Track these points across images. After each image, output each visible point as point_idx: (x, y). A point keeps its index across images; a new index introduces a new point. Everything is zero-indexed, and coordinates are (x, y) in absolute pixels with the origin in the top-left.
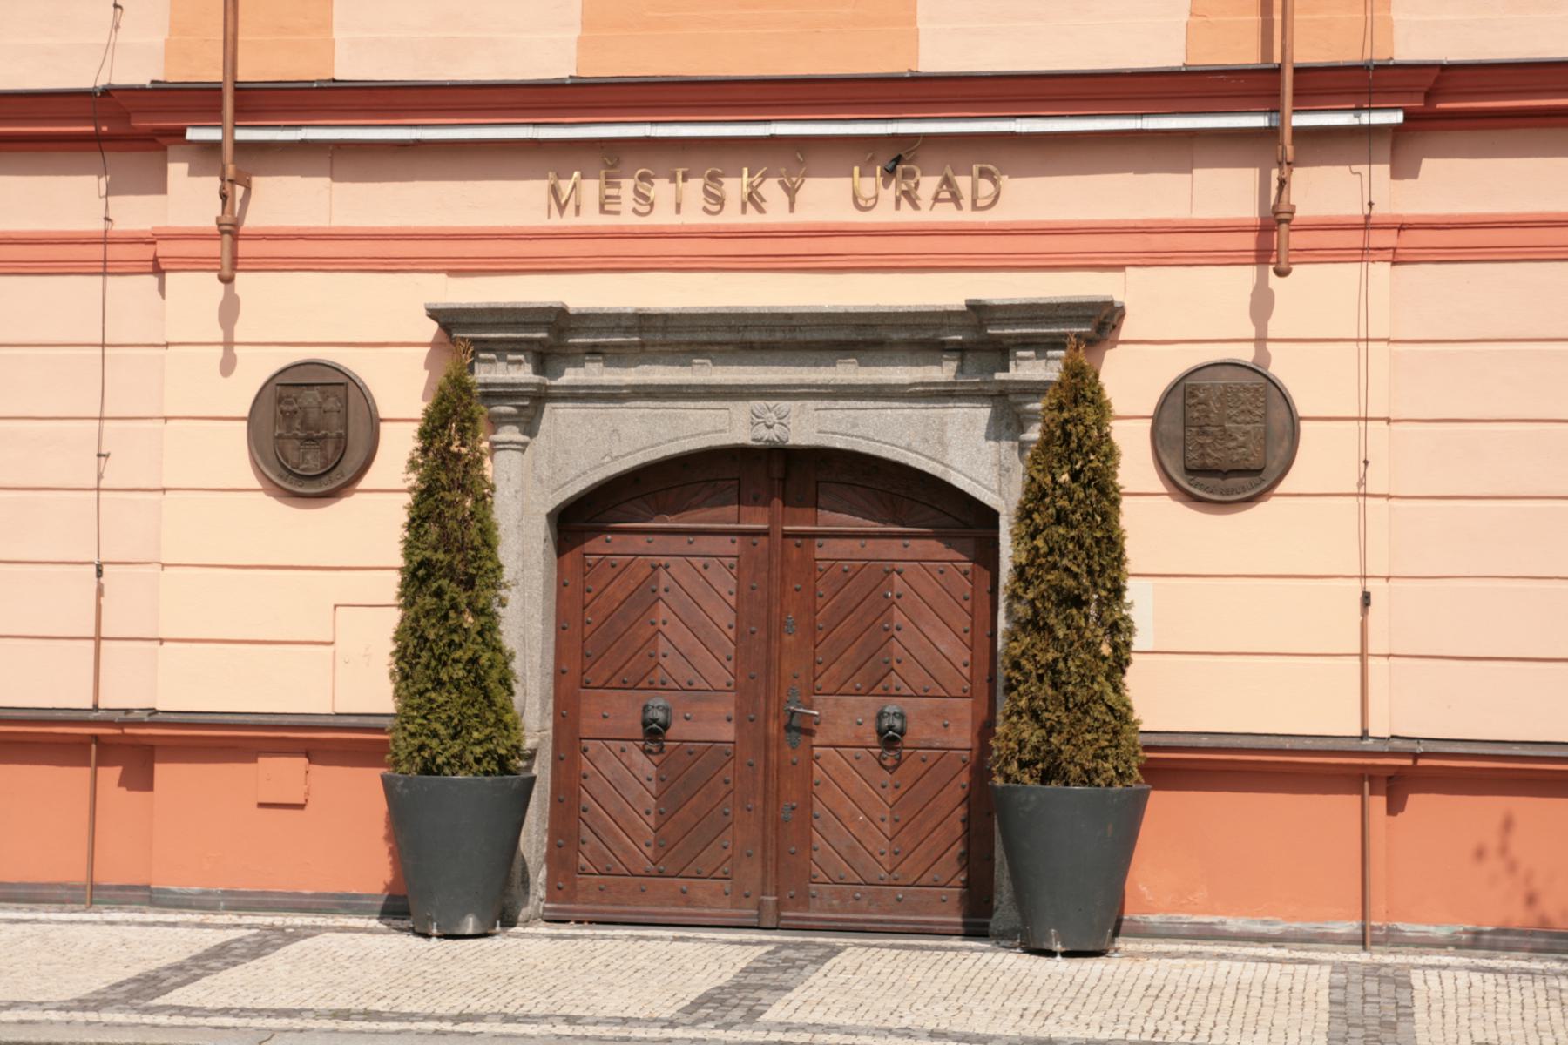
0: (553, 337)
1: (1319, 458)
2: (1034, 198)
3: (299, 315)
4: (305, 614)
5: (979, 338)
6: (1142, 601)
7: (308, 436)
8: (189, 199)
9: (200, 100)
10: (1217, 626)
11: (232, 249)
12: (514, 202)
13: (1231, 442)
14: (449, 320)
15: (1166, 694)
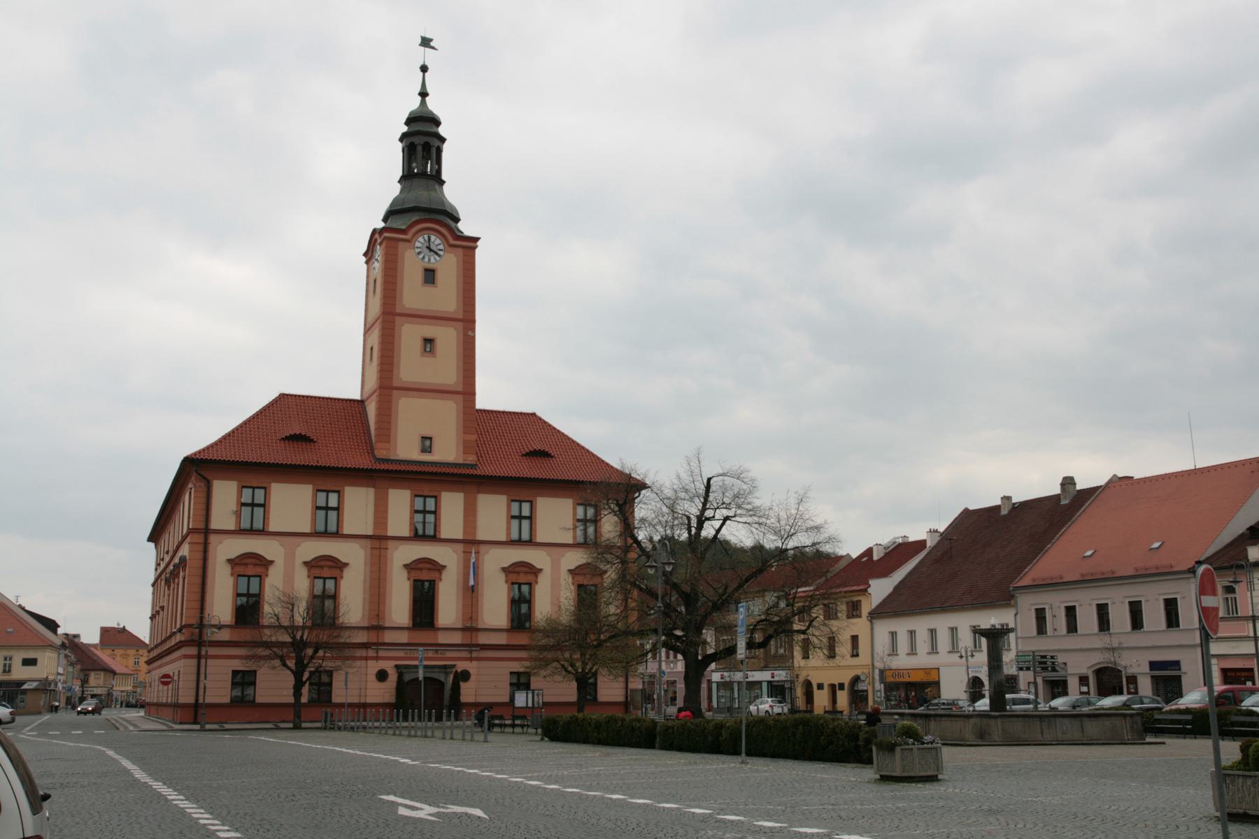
0: (407, 667)
1: (473, 678)
2: (449, 654)
3: (383, 665)
4: (383, 693)
5: (445, 667)
6: (462, 691)
7: (382, 676)
8: (371, 653)
9: (375, 644)
10: (468, 693)
11: (377, 658)
12: (401, 654)
13: (465, 676)
14: (396, 666)
15: (464, 699)
